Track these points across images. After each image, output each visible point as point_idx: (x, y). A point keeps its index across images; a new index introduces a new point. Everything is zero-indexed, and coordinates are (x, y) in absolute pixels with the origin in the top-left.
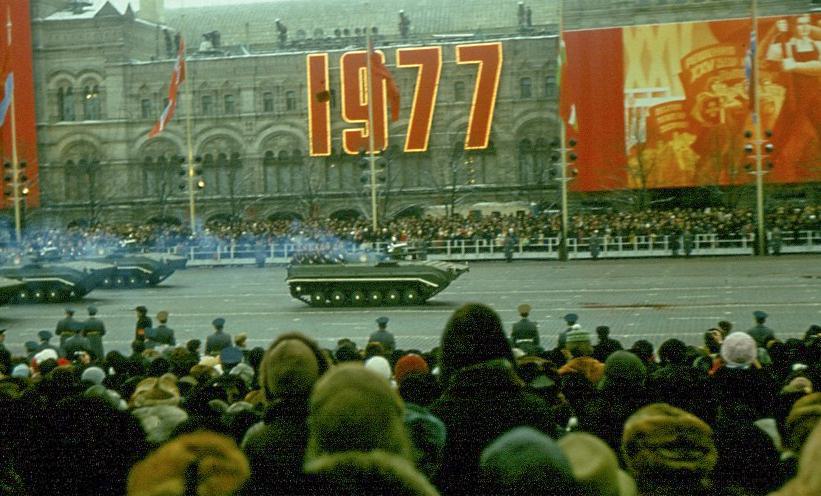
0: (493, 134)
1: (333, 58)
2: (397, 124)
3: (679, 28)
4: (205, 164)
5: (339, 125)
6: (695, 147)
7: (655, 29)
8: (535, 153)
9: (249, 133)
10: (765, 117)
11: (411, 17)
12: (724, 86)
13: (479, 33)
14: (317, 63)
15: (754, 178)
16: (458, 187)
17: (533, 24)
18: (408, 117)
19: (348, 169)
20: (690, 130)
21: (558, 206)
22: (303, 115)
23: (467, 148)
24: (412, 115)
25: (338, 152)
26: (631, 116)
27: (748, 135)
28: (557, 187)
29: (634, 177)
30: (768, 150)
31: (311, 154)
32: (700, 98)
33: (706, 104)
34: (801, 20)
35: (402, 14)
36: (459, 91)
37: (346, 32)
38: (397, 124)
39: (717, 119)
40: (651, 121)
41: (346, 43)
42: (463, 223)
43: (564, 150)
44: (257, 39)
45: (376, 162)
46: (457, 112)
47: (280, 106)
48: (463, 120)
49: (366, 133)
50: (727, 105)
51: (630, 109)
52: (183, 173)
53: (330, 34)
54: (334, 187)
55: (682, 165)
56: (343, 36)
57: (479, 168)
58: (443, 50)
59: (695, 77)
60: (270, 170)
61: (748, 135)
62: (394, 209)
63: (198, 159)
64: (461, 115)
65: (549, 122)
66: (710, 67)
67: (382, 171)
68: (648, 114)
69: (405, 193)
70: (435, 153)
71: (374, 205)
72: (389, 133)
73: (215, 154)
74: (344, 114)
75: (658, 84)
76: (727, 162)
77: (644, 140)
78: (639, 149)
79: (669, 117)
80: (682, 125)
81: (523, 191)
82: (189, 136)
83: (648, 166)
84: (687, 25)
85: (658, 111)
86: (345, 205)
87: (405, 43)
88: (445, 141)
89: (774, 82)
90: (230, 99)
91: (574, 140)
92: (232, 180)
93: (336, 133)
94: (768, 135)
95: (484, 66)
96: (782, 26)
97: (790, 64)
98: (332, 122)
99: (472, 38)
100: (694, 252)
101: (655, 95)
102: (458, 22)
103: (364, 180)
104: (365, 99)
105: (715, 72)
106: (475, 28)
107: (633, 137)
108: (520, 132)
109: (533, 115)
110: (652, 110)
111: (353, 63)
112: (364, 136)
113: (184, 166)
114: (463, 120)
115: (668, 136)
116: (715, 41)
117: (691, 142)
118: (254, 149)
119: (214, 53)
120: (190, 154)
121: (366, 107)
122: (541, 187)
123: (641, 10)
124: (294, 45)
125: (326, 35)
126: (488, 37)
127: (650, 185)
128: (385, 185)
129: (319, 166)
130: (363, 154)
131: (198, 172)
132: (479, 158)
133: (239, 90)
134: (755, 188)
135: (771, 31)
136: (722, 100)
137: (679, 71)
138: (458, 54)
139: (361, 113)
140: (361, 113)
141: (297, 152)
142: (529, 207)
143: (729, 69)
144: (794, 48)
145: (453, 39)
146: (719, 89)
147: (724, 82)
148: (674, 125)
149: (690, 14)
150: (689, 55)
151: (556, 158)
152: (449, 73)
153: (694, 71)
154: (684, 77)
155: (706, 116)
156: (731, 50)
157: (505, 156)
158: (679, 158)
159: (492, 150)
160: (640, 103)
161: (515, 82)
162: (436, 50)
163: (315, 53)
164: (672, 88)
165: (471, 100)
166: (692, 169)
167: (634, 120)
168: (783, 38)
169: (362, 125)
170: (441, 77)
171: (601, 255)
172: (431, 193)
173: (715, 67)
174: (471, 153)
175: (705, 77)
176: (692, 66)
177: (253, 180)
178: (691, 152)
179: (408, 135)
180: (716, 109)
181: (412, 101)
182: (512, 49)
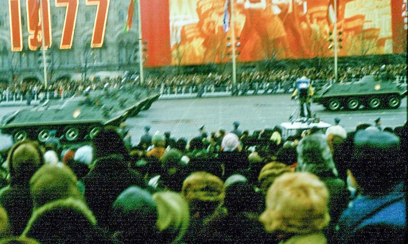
5: (26, 34)
6: (205, 44)
8: (126, 47)
10: (236, 30)
12: (217, 15)
15: (231, 60)
16: (88, 66)
19: (32, 57)
21: (138, 73)
25: (26, 48)
27: (229, 39)
28: (137, 65)
32: (206, 21)
36: (87, 17)
40: (183, 32)
42: (90, 84)
46: (86, 28)
54: (24, 66)
55: (198, 53)
57: (99, 55)
59: (203, 11)
62: (55, 76)
65: (132, 33)
66: (210, 6)
70: (75, 49)
72: (53, 38)
76: (218, 52)
78: (177, 46)
81: (121, 67)
85: (186, 28)
86: (30, 75)
88: (81, 42)
89: (240, 13)
91: (146, 40)
93: (25, 38)
94: (238, 39)
98: (23, 33)
103: (40, 62)
105: (213, 9)
108: (119, 37)
114: (90, 32)
115: (191, 40)
122: (129, 64)
127: (182, 62)
129: (17, 56)
130: (39, 49)
132: (98, 51)
134: (231, 64)
136: (216, 23)
141: (5, 48)
142: (124, 74)
151: (137, 50)
154: (199, 11)
158: (196, 50)
159: (105, 46)
161: (116, 13)
166: (203, 54)
167: (174, 33)
174: (93, 49)
176: (201, 7)
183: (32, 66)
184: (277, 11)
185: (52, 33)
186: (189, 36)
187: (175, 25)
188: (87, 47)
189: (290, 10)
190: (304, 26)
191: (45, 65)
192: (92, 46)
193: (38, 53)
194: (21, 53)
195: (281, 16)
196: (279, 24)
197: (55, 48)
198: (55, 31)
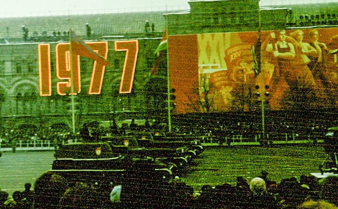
0: (134, 85)
1: (52, 47)
3: (224, 35)
6: (232, 92)
7: (213, 36)
9: (9, 83)
12: (246, 64)
13: (127, 36)
14: (44, 49)
16: (116, 112)
18: (91, 77)
19: (60, 102)
20: (230, 85)
22: (37, 75)
23: (121, 92)
24: (93, 75)
26: (201, 78)
28: (166, 112)
29: (203, 108)
34: (282, 33)
35: (87, 26)
36: (117, 63)
37: (59, 33)
39: (242, 81)
40: (210, 79)
41: (58, 39)
43: (169, 94)
44: (14, 36)
45: (75, 99)
46: (116, 74)
47: (24, 69)
48: (118, 78)
50: (247, 73)
51: (201, 74)
55: (226, 102)
56: (57, 35)
58: (108, 43)
60: (20, 102)
61: (257, 87)
64: (118, 76)
66: (239, 55)
67: (78, 103)
68: (209, 77)
69: (91, 115)
71: (74, 121)
72: (82, 84)
74: (58, 75)
77: (208, 89)
78: (206, 93)
79: (219, 79)
80: (226, 82)
81: (150, 114)
83: (209, 102)
84: (228, 34)
85: (215, 75)
87: (89, 39)
88: (109, 89)
89: (269, 62)
93: (54, 84)
94: (267, 87)
96: (273, 35)
97: (277, 54)
98: (52, 79)
99: (123, 38)
100: (232, 144)
101: (213, 67)
102: (115, 29)
103: (68, 108)
104: (69, 68)
105: (242, 57)
106: (125, 33)
107: (202, 88)
110: (212, 75)
111: (63, 49)
112: (68, 86)
115: (218, 88)
116: (241, 43)
117: (230, 91)
118: (11, 92)
121: (69, 72)
123: (205, 27)
124: (32, 39)
125: (48, 35)
126: (131, 38)
128: (79, 111)
130: (68, 95)
133: (4, 61)
135: (268, 37)
136: (244, 70)
137: (225, 56)
139: (67, 74)
140: (67, 74)
144: (278, 46)
145: (113, 38)
146: (243, 65)
150: (229, 49)
151: (166, 97)
152: (112, 55)
153: (232, 56)
154: (227, 59)
158: (224, 97)
159: (133, 94)
160: (206, 71)
161: (145, 60)
163: (43, 44)
165: (123, 68)
167: (203, 79)
169: (67, 80)
172: (102, 114)
173: (241, 54)
174: (122, 95)
176: (230, 54)
178: (230, 95)
179: (91, 85)
180: (242, 75)
181: (92, 70)
182: (143, 44)
183: (61, 111)
184: (307, 60)
186: (217, 84)
187: (204, 73)
188: (116, 94)
189: (320, 60)
191: (73, 111)
192: (121, 92)
194: (49, 98)
195: (310, 66)
197: (83, 95)
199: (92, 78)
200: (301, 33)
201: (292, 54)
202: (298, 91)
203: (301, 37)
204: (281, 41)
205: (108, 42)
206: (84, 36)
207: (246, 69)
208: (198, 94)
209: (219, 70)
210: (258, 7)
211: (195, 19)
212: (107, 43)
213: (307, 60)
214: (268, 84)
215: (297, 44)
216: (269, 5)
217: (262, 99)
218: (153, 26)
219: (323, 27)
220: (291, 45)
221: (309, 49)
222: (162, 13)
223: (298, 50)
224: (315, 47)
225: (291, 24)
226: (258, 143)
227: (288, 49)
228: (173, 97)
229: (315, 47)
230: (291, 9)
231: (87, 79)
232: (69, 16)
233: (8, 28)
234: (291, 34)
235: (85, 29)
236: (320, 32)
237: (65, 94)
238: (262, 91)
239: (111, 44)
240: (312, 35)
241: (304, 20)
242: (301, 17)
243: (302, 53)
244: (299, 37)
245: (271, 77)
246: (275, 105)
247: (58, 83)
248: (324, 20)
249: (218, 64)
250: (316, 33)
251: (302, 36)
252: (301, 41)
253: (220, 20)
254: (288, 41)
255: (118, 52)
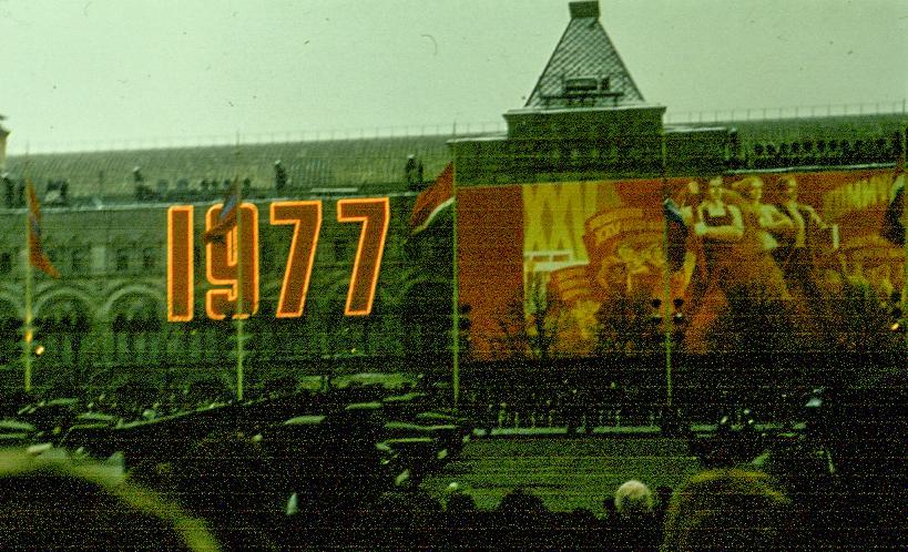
0: (377, 300)
1: (199, 214)
2: (268, 286)
3: (583, 188)
4: (45, 328)
5: (203, 286)
11: (290, 170)
12: (631, 251)
13: (365, 189)
14: (180, 218)
16: (336, 356)
17: (425, 180)
18: (282, 277)
19: (211, 334)
20: (594, 296)
21: (449, 379)
22: (163, 274)
27: (657, 303)
30: (677, 321)
31: (171, 317)
32: (605, 263)
33: (612, 268)
35: (278, 166)
37: (215, 184)
38: (268, 286)
39: (623, 287)
43: (456, 317)
44: (114, 190)
46: (338, 273)
47: (135, 262)
48: (344, 282)
49: (233, 296)
50: (634, 272)
51: (530, 274)
52: (21, 338)
53: (195, 185)
55: (585, 334)
59: (600, 239)
60: (123, 335)
61: (657, 303)
63: (37, 322)
68: (548, 279)
71: (240, 376)
72: (261, 294)
73: (58, 317)
75: (561, 247)
79: (571, 283)
80: (585, 292)
81: (409, 363)
82: (28, 297)
85: (561, 277)
90: (78, 256)
92: (76, 347)
93: (200, 295)
94: (678, 303)
95: (368, 224)
96: (693, 187)
97: (701, 229)
99: (356, 194)
102: (340, 175)
103: (230, 347)
104: (233, 259)
105: (623, 235)
106: (363, 179)
109: (421, 279)
110: (554, 274)
112: (231, 299)
113: (20, 331)
114: (344, 282)
115: (569, 305)
118: (103, 312)
119: (63, 204)
120: (29, 319)
125: (190, 187)
129: (179, 333)
130: (228, 319)
131: (36, 337)
133: (89, 247)
135: (682, 193)
137: (582, 233)
138: (339, 209)
140: (231, 273)
143: (637, 233)
144: (706, 213)
145: (334, 194)
146: (626, 255)
147: (631, 246)
148: (577, 292)
149: (596, 174)
151: (449, 324)
153: (599, 234)
154: (588, 239)
155: (613, 285)
156: (639, 212)
157: (388, 321)
160: (539, 267)
162: (316, 206)
163: (178, 207)
164: (575, 248)
165: (353, 261)
168: (694, 201)
169: (230, 286)
170: (321, 236)
171: (494, 432)
174: (352, 320)
175: (611, 240)
177: (103, 344)
182: (400, 205)
184: (770, 243)
185: (261, 284)
186: (566, 297)
188: (335, 316)
189: (800, 244)
190: (835, 279)
191: (240, 354)
192: (347, 313)
193: (227, 327)
194: (187, 326)
195: (777, 254)
196: (777, 276)
198: (267, 280)
199: (285, 282)
200: (757, 183)
201: (736, 229)
202: (748, 312)
203: (758, 194)
204: (714, 202)
205: (323, 201)
206: (270, 189)
207: (633, 265)
208: (521, 316)
209: (572, 262)
210: (660, 125)
211: (517, 152)
212: (319, 203)
213: (770, 243)
214: (681, 294)
215: (750, 209)
216: (687, 121)
217: (668, 329)
218: (421, 170)
219: (806, 171)
220: (734, 210)
221: (776, 219)
222: (446, 137)
223: (751, 220)
224: (791, 217)
225: (736, 163)
226: (658, 429)
227: (727, 220)
228: (464, 325)
229: (791, 217)
230: (734, 130)
231: (274, 284)
232: (237, 147)
233: (101, 175)
234: (735, 185)
235: (272, 173)
236: (802, 182)
237: (222, 317)
238: (667, 311)
239: (329, 207)
240: (783, 187)
241: (765, 156)
242: (759, 149)
243: (758, 227)
244: (753, 192)
245: (688, 281)
246: (697, 345)
247: (209, 293)
248: (810, 155)
249: (568, 251)
250: (793, 183)
251: (760, 191)
252: (757, 202)
253: (575, 154)
254: (727, 201)
255: (345, 224)
